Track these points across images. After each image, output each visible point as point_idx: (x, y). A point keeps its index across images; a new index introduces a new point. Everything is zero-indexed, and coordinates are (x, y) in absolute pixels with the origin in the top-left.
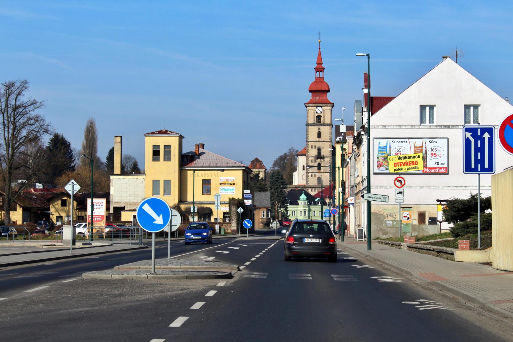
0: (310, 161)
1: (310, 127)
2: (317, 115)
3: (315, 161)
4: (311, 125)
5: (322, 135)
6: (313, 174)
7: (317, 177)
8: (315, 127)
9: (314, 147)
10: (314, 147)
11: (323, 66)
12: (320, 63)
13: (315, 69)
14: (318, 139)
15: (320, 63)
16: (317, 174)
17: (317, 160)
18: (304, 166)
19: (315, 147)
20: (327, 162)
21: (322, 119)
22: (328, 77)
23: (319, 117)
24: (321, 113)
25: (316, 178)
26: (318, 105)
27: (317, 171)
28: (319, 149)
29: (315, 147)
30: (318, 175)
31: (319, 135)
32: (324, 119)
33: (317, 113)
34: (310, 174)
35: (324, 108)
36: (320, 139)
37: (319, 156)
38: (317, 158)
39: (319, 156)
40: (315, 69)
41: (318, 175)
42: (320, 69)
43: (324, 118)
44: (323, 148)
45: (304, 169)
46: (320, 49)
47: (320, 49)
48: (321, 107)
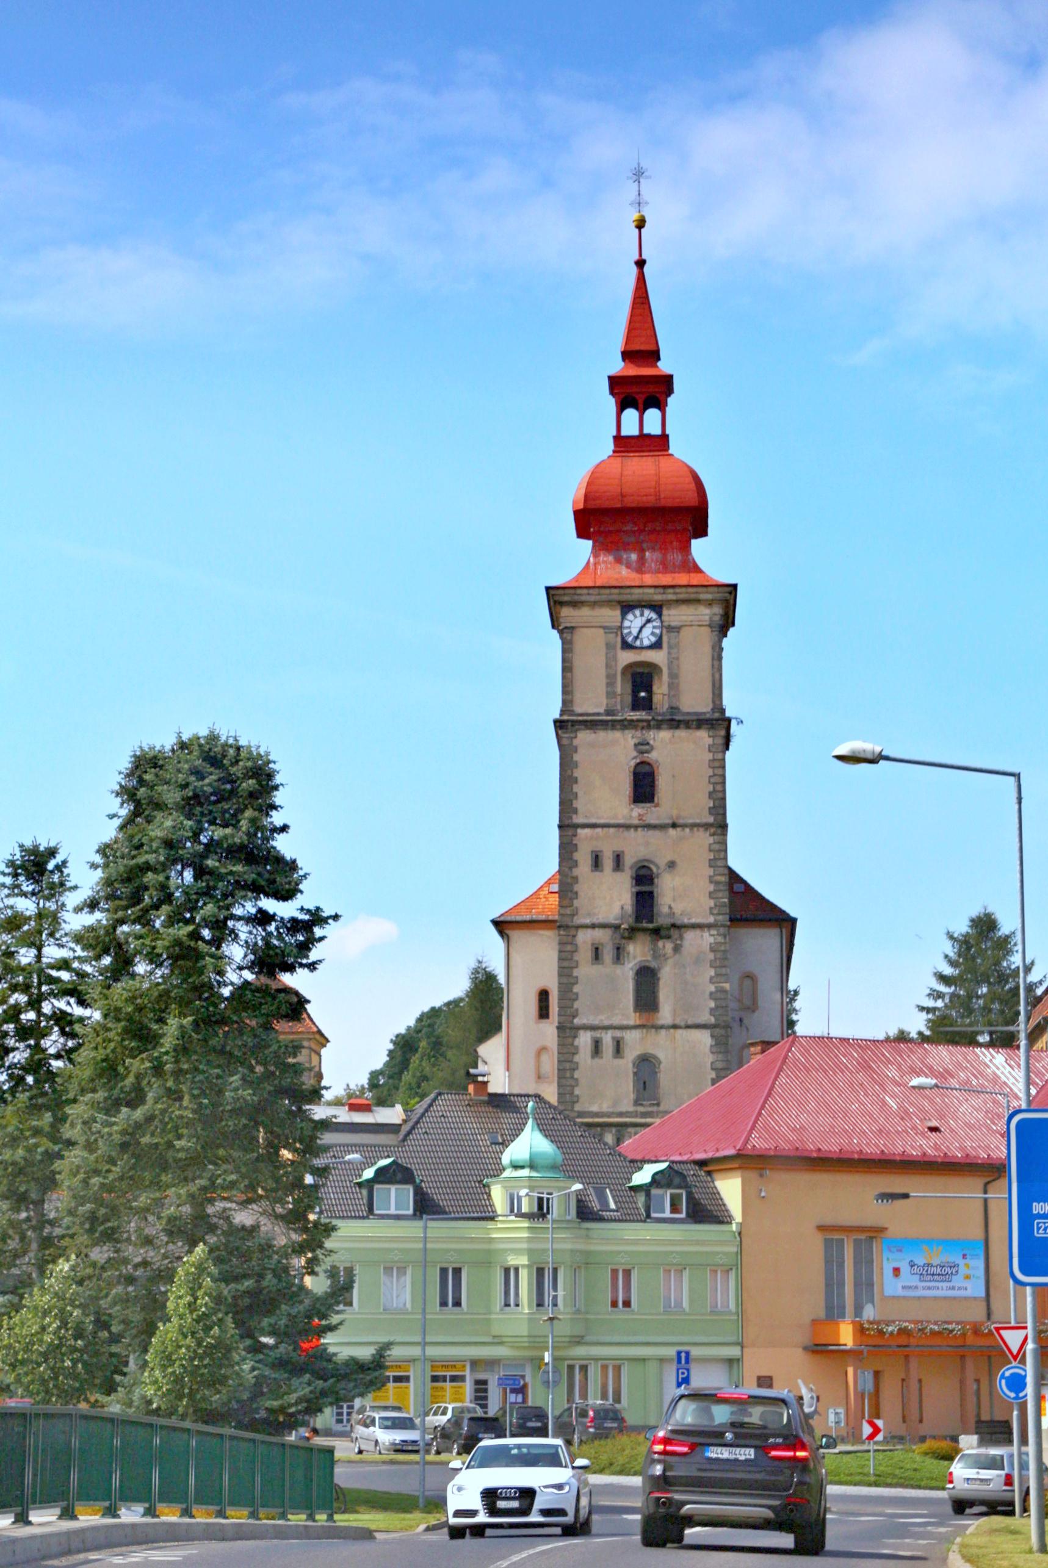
1: (584, 737)
2: (627, 658)
3: (619, 954)
4: (592, 724)
5: (663, 783)
6: (607, 1038)
7: (631, 1053)
8: (617, 735)
9: (608, 862)
10: (608, 862)
11: (665, 366)
12: (641, 347)
14: (638, 810)
15: (641, 347)
16: (631, 1038)
18: (544, 996)
19: (618, 859)
20: (697, 961)
21: (660, 689)
22: (695, 432)
23: (641, 679)
24: (657, 645)
27: (633, 1019)
28: (644, 880)
29: (618, 859)
30: (636, 1043)
31: (644, 786)
32: (673, 686)
34: (584, 1040)
35: (673, 615)
37: (646, 916)
38: (632, 932)
39: (646, 916)
41: (636, 1043)
42: (642, 385)
43: (674, 676)
44: (672, 865)
45: (543, 1012)
46: (641, 263)
47: (641, 263)
48: (657, 608)
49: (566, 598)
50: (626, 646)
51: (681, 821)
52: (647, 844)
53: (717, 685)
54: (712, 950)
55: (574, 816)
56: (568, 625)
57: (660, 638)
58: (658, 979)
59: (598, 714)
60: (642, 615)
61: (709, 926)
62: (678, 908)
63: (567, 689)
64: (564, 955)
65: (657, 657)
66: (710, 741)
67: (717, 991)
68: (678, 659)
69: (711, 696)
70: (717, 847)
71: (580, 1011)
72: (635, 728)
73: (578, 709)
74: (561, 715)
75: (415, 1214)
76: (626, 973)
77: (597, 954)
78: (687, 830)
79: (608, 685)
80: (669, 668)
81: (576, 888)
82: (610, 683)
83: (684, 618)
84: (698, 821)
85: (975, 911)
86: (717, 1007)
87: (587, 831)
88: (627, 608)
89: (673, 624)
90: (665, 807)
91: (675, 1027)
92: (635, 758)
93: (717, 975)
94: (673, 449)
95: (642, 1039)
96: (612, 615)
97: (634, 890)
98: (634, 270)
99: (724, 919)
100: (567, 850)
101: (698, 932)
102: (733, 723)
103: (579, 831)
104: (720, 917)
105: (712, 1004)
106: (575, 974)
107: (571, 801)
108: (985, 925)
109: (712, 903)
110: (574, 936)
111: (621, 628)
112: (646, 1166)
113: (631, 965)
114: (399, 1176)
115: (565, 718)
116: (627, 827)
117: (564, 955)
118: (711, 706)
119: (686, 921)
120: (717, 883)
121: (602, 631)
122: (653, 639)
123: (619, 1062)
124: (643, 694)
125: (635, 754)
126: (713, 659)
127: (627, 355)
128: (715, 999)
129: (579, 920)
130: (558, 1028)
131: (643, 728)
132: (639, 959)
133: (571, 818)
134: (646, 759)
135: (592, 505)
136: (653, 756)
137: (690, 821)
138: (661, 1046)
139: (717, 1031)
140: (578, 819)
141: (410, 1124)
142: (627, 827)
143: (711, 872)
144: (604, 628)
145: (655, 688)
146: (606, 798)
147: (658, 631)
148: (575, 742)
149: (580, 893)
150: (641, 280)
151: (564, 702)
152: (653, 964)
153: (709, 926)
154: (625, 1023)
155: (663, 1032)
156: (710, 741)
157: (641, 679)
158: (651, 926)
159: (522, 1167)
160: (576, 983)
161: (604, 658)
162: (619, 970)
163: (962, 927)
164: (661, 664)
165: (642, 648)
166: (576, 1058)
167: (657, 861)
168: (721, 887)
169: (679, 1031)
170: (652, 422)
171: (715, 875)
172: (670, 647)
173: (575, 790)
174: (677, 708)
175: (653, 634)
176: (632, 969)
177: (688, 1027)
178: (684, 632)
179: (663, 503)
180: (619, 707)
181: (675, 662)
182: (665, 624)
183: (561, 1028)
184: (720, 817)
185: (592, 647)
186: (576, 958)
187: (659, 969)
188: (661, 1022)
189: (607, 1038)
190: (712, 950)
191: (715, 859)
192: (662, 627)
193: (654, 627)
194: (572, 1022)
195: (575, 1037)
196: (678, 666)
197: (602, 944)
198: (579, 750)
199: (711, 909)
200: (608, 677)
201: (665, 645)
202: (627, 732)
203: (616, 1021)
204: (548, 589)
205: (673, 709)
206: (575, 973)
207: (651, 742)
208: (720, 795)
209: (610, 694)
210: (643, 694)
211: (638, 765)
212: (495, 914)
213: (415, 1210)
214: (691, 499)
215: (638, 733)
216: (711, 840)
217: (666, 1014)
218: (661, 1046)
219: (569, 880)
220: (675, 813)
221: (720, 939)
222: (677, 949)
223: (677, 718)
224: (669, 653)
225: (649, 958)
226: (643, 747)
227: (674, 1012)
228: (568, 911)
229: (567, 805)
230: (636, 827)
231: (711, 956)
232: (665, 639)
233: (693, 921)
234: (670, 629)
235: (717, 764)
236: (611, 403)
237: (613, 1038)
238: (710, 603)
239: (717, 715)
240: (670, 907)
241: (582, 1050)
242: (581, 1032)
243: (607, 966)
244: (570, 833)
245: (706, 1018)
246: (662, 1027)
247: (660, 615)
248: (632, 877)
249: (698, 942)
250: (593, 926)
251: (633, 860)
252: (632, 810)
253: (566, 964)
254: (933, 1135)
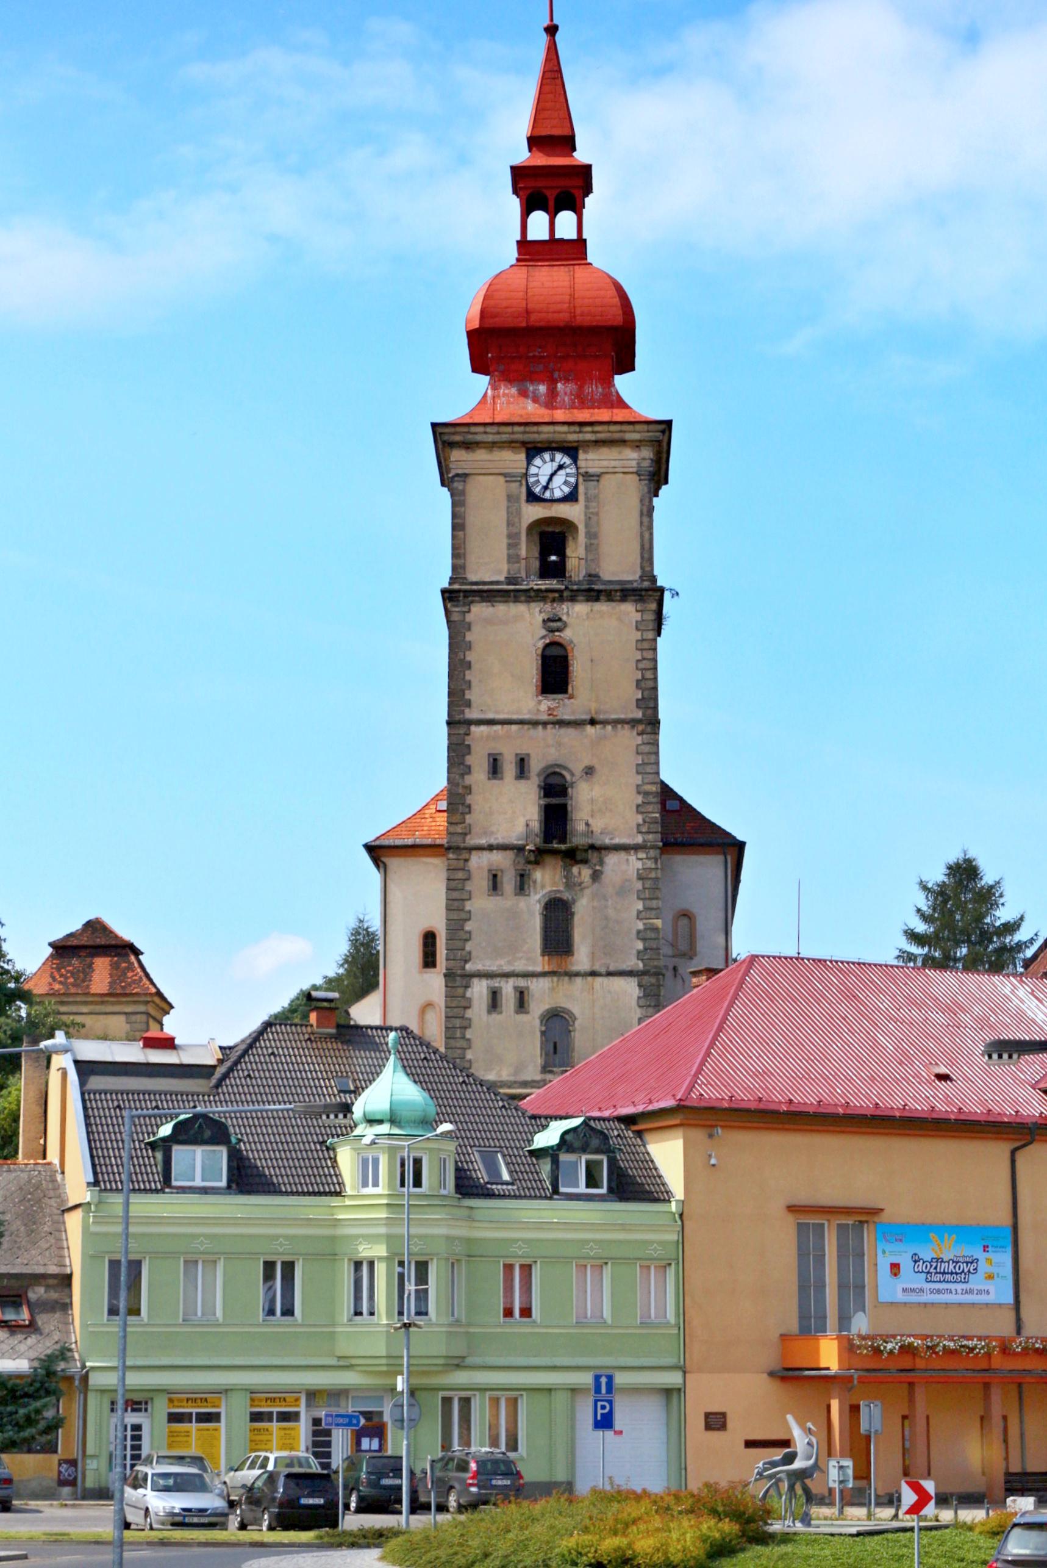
0: (479, 883)
1: (479, 611)
2: (533, 512)
3: (523, 884)
4: (490, 595)
5: (579, 669)
6: (508, 988)
7: (538, 1007)
8: (521, 608)
9: (509, 769)
10: (509, 769)
11: (581, 156)
12: (553, 133)
13: (518, 173)
14: (547, 703)
15: (553, 133)
16: (538, 987)
17: (538, 875)
18: (429, 938)
19: (522, 763)
20: (622, 891)
23: (552, 539)
24: (571, 497)
25: (532, 1020)
27: (540, 964)
29: (522, 763)
31: (555, 672)
33: (532, 498)
34: (479, 990)
35: (590, 460)
36: (567, 708)
37: (557, 835)
38: (539, 856)
39: (557, 835)
40: (518, 173)
42: (553, 179)
43: (592, 535)
44: (589, 771)
45: (429, 961)
46: (552, 30)
47: (552, 30)
48: (571, 451)
49: (457, 438)
50: (532, 498)
51: (601, 717)
52: (559, 744)
53: (647, 546)
54: (640, 878)
55: (467, 710)
56: (460, 472)
57: (576, 486)
58: (572, 914)
59: (497, 583)
60: (552, 460)
61: (636, 848)
62: (597, 825)
63: (458, 552)
64: (453, 884)
65: (572, 512)
66: (638, 616)
67: (645, 929)
68: (597, 514)
69: (639, 561)
70: (646, 749)
71: (474, 954)
72: (544, 599)
73: (472, 577)
74: (450, 584)
75: (229, 1187)
76: (532, 907)
77: (495, 883)
78: (609, 728)
79: (510, 546)
80: (587, 526)
81: (469, 799)
82: (513, 545)
83: (605, 463)
84: (622, 716)
85: (954, 856)
86: (646, 949)
87: (483, 729)
88: (533, 450)
89: (591, 471)
91: (594, 974)
92: (543, 637)
93: (647, 909)
94: (593, 255)
95: (553, 989)
96: (515, 460)
97: (542, 802)
98: (544, 38)
99: (654, 838)
100: (458, 754)
101: (623, 855)
102: (667, 595)
103: (473, 728)
104: (651, 837)
105: (640, 946)
106: (467, 908)
107: (463, 691)
108: (964, 871)
109: (640, 819)
110: (466, 860)
111: (526, 475)
112: (554, 1124)
113: (538, 897)
114: (208, 1134)
115: (456, 587)
116: (535, 723)
117: (453, 884)
118: (639, 573)
119: (607, 841)
120: (646, 794)
121: (502, 479)
122: (567, 490)
123: (522, 1017)
124: (553, 558)
125: (544, 632)
126: (642, 514)
127: (534, 142)
128: (644, 940)
129: (472, 841)
130: (445, 975)
131: (553, 600)
132: (548, 889)
133: (463, 712)
134: (557, 639)
135: (491, 323)
136: (567, 635)
137: (614, 716)
138: (575, 997)
139: (646, 979)
140: (472, 714)
141: (228, 1064)
142: (535, 723)
143: (638, 779)
144: (505, 475)
145: (569, 552)
146: (509, 687)
147: (572, 480)
148: (469, 618)
149: (473, 807)
150: (552, 52)
151: (454, 568)
152: (566, 896)
153: (636, 848)
154: (531, 969)
155: (579, 980)
156: (638, 616)
157: (552, 539)
158: (563, 847)
159: (380, 1122)
160: (469, 919)
161: (504, 514)
162: (522, 903)
163: (937, 875)
164: (576, 521)
165: (553, 501)
166: (469, 1014)
167: (570, 766)
168: (651, 799)
169: (599, 980)
170: (566, 225)
171: (644, 783)
172: (587, 500)
173: (467, 678)
174: (597, 576)
175: (566, 483)
176: (539, 901)
177: (610, 974)
178: (606, 480)
179: (579, 321)
180: (523, 575)
181: (594, 518)
182: (582, 471)
183: (449, 976)
184: (650, 712)
185: (490, 497)
186: (468, 888)
187: (574, 901)
188: (575, 968)
189: (508, 988)
190: (640, 878)
191: (644, 764)
192: (578, 474)
193: (567, 475)
194: (464, 968)
195: (467, 987)
196: (598, 523)
197: (502, 871)
198: (473, 628)
199: (639, 825)
200: (510, 536)
202: (533, 605)
203: (520, 966)
204: (434, 425)
205: (593, 577)
206: (468, 906)
207: (564, 618)
208: (650, 684)
209: (512, 559)
210: (553, 558)
211: (547, 646)
212: (369, 838)
213: (230, 1181)
214: (616, 317)
215: (548, 607)
216: (639, 740)
217: (581, 959)
218: (575, 997)
219: (460, 791)
220: (594, 706)
221: (650, 864)
222: (596, 876)
223: (596, 587)
224: (587, 507)
225: (562, 888)
226: (553, 623)
227: (593, 956)
228: (459, 829)
229: (457, 696)
230: (545, 724)
231: (639, 885)
233: (617, 841)
234: (588, 477)
235: (646, 645)
236: (514, 204)
237: (515, 988)
238: (637, 445)
239: (646, 584)
240: (587, 824)
241: (475, 1003)
242: (475, 981)
243: (508, 900)
244: (462, 732)
245: (633, 963)
246: (577, 974)
247: (575, 459)
248: (539, 786)
249: (623, 869)
250: (491, 848)
251: (542, 765)
252: (540, 702)
253: (456, 895)
254: (942, 1085)
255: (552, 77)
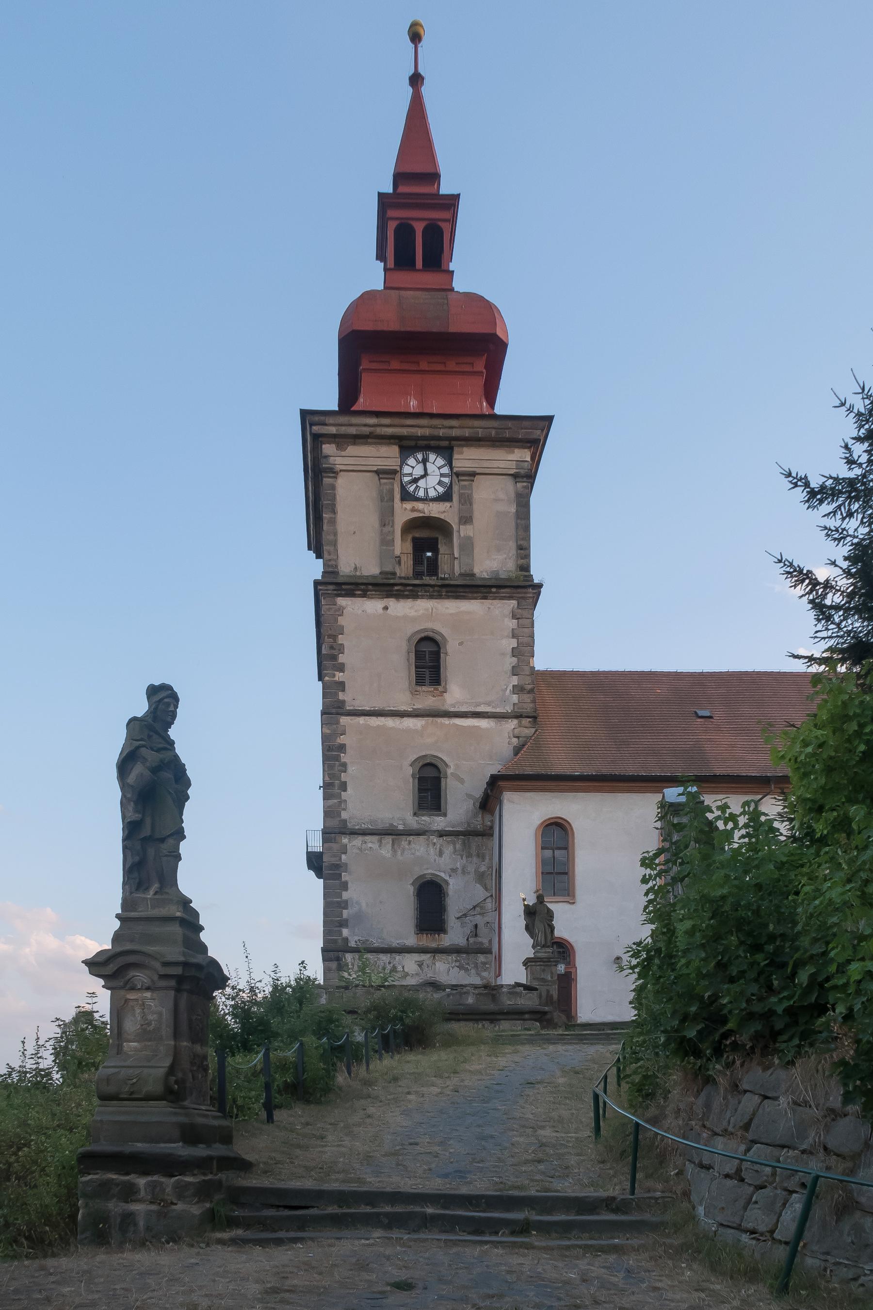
26: (421, 429)
33: (407, 496)
35: (467, 458)
46: (416, 80)
47: (416, 80)
50: (407, 496)
57: (450, 487)
90: (455, 694)
122: (441, 490)
124: (429, 554)
165: (426, 500)
175: (440, 483)
182: (455, 470)
201: (455, 497)
210: (429, 554)
232: (456, 488)
255: (416, 115)
